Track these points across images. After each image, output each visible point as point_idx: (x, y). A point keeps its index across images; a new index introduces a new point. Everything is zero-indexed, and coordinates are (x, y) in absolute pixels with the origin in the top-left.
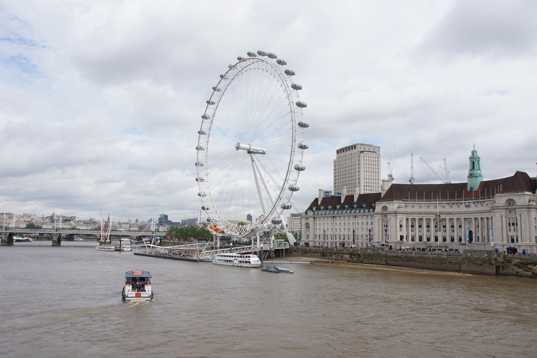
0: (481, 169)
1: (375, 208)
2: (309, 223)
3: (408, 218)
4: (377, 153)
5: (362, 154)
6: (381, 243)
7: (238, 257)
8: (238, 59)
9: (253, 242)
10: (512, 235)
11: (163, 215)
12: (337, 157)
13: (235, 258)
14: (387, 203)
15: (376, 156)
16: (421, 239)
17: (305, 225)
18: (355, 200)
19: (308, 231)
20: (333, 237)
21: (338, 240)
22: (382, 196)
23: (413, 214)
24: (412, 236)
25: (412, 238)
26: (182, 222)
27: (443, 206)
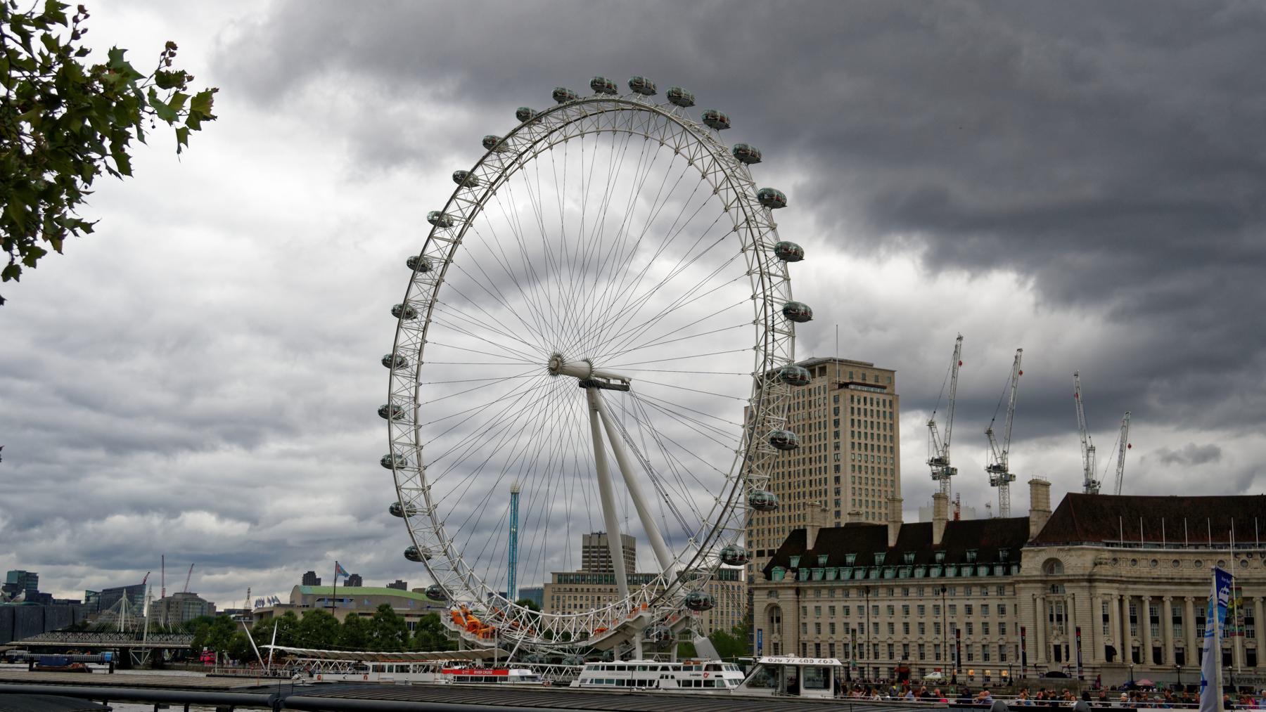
1: (1019, 566)
2: (780, 604)
6: (1046, 669)
8: (555, 95)
11: (21, 575)
14: (1061, 550)
16: (1158, 655)
18: (937, 539)
19: (776, 630)
20: (866, 652)
21: (884, 658)
22: (1034, 530)
23: (1135, 583)
24: (1133, 648)
25: (1133, 653)
26: (88, 598)
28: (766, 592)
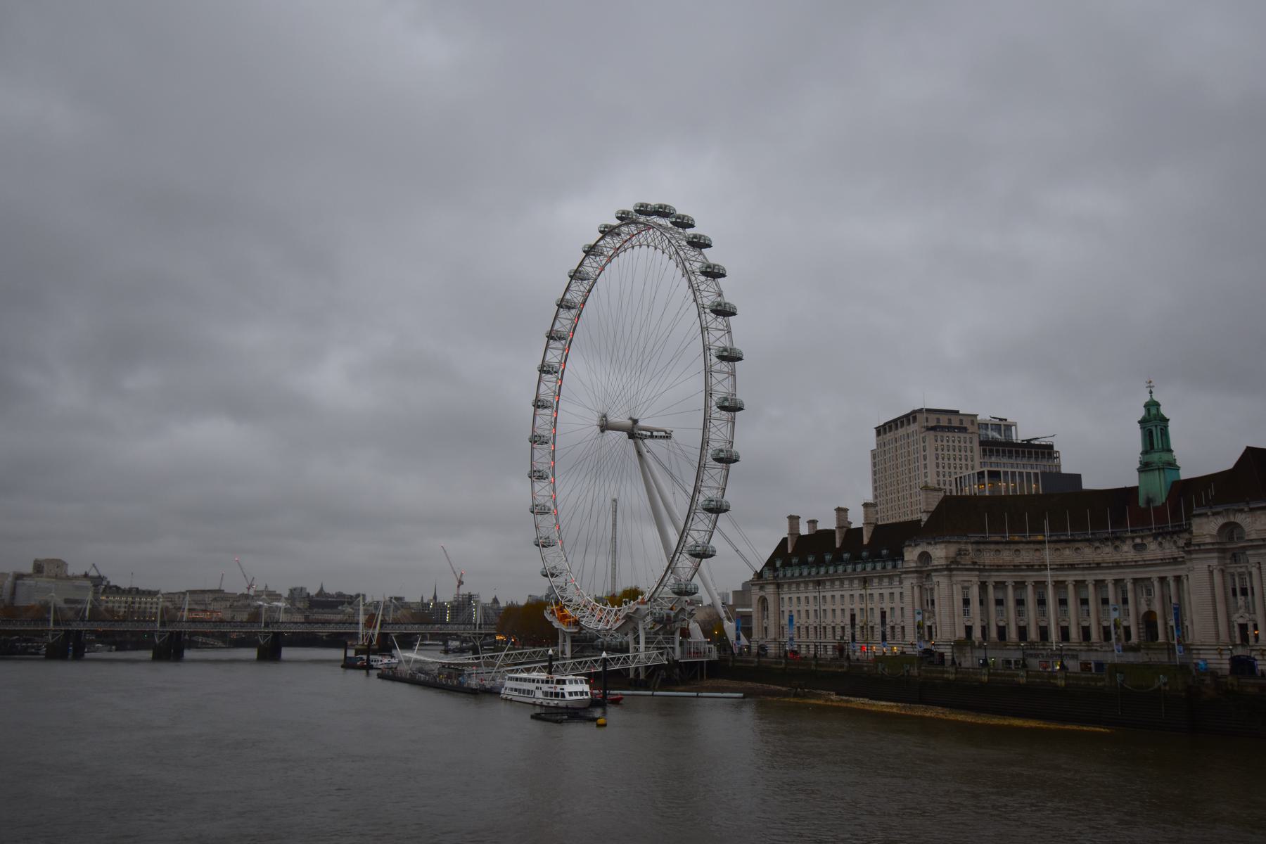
0: (1172, 448)
1: (903, 560)
2: (767, 596)
3: (985, 582)
4: (970, 431)
5: (932, 432)
7: (543, 682)
9: (632, 646)
10: (1241, 621)
12: (877, 444)
13: (538, 685)
14: (929, 544)
15: (965, 438)
17: (760, 603)
18: (866, 541)
19: (766, 617)
24: (1001, 627)
27: (1078, 548)
28: (757, 587)
